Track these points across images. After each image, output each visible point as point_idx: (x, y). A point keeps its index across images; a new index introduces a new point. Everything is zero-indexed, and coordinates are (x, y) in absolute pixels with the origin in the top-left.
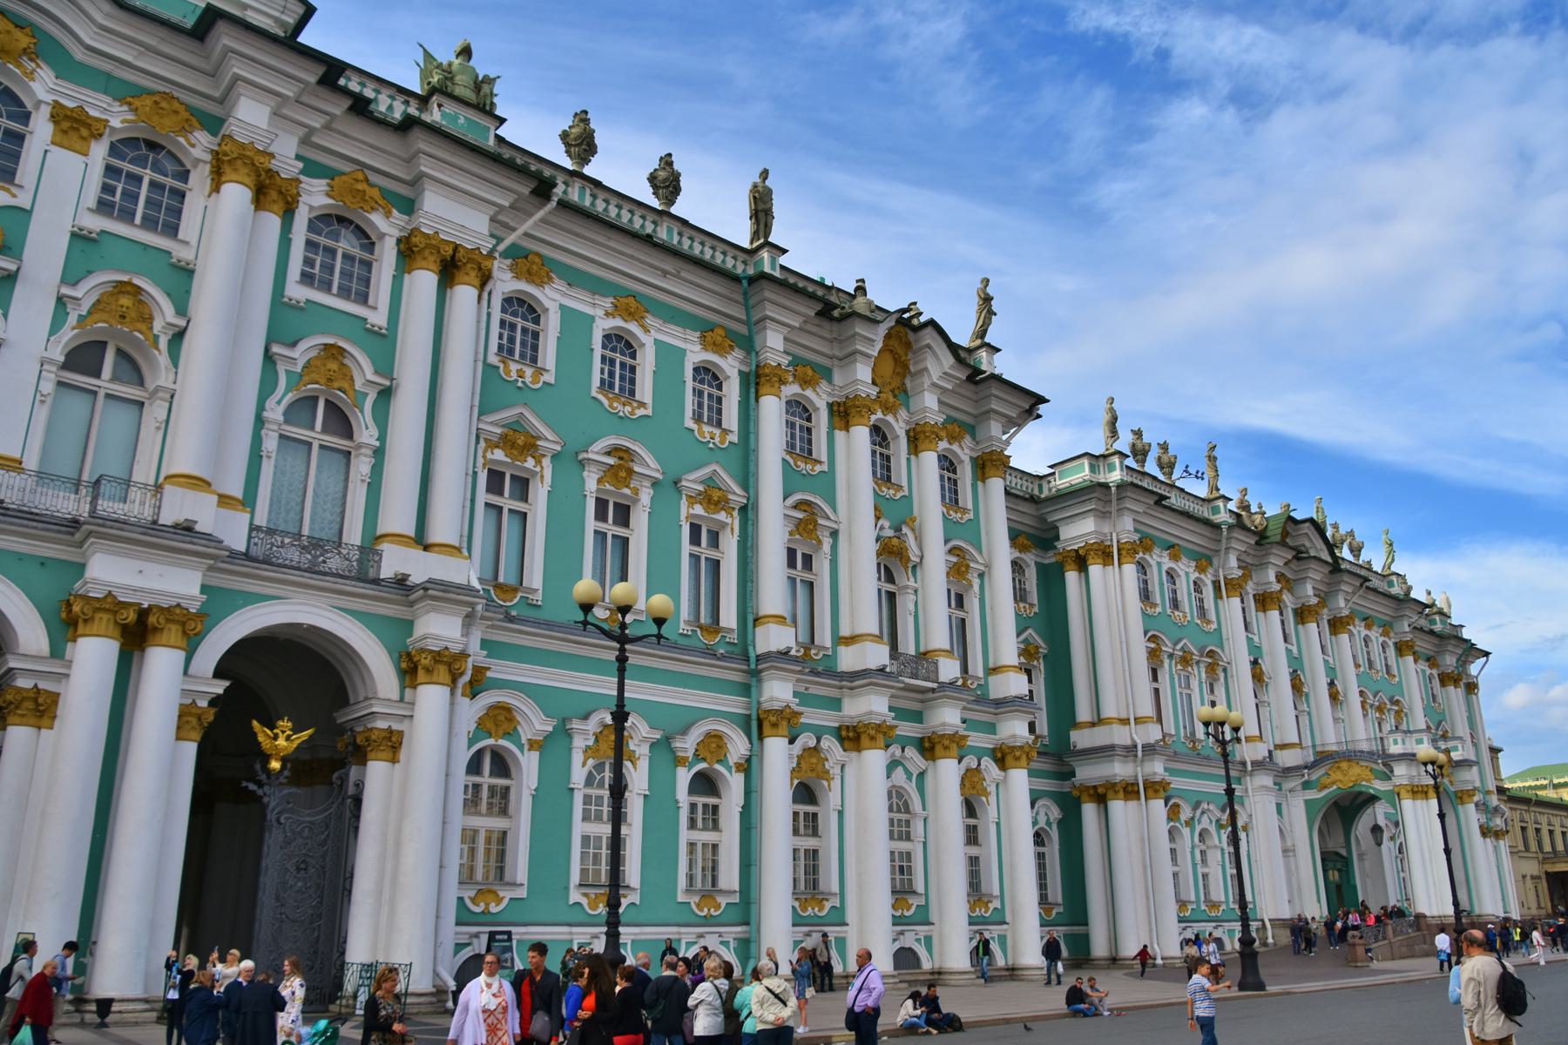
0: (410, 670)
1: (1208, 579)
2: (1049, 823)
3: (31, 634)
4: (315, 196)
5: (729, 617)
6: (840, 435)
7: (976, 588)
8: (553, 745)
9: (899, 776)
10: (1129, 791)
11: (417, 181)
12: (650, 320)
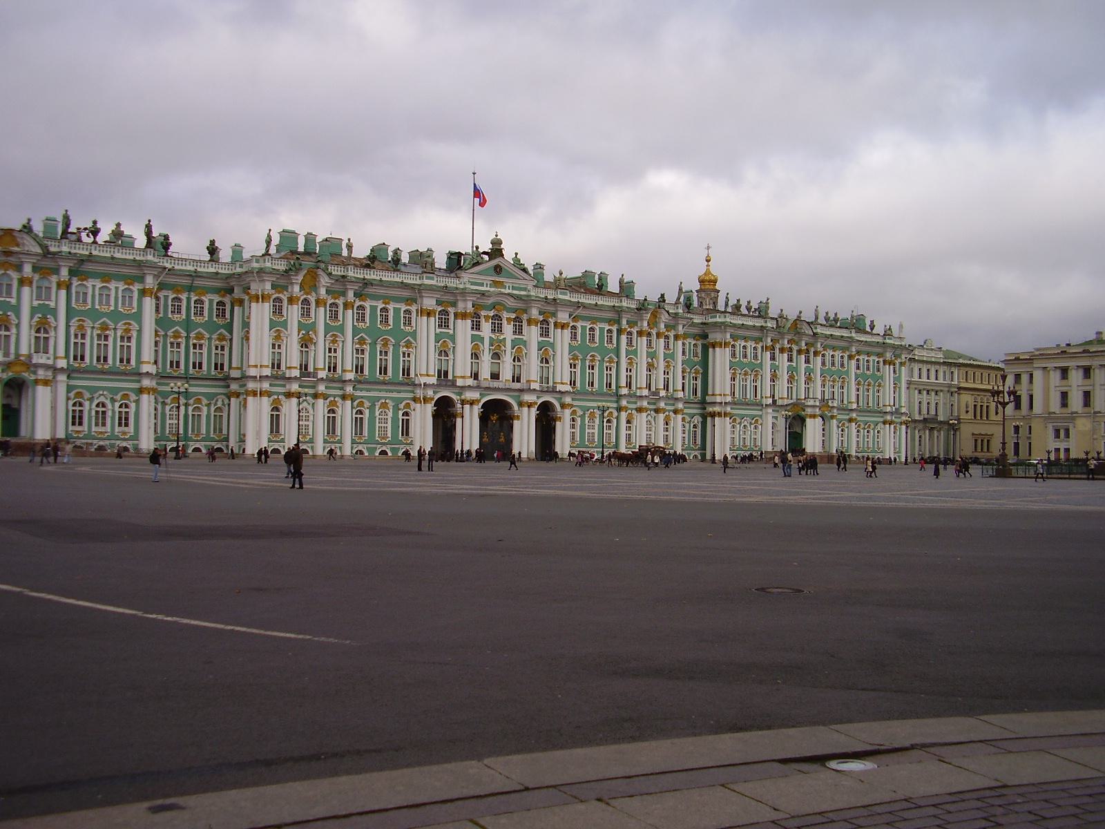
0: (563, 406)
1: (759, 346)
2: (698, 422)
3: (516, 407)
4: (541, 318)
5: (614, 386)
6: (639, 338)
7: (672, 370)
8: (582, 417)
9: (649, 417)
10: (719, 414)
11: (557, 311)
12: (598, 323)
